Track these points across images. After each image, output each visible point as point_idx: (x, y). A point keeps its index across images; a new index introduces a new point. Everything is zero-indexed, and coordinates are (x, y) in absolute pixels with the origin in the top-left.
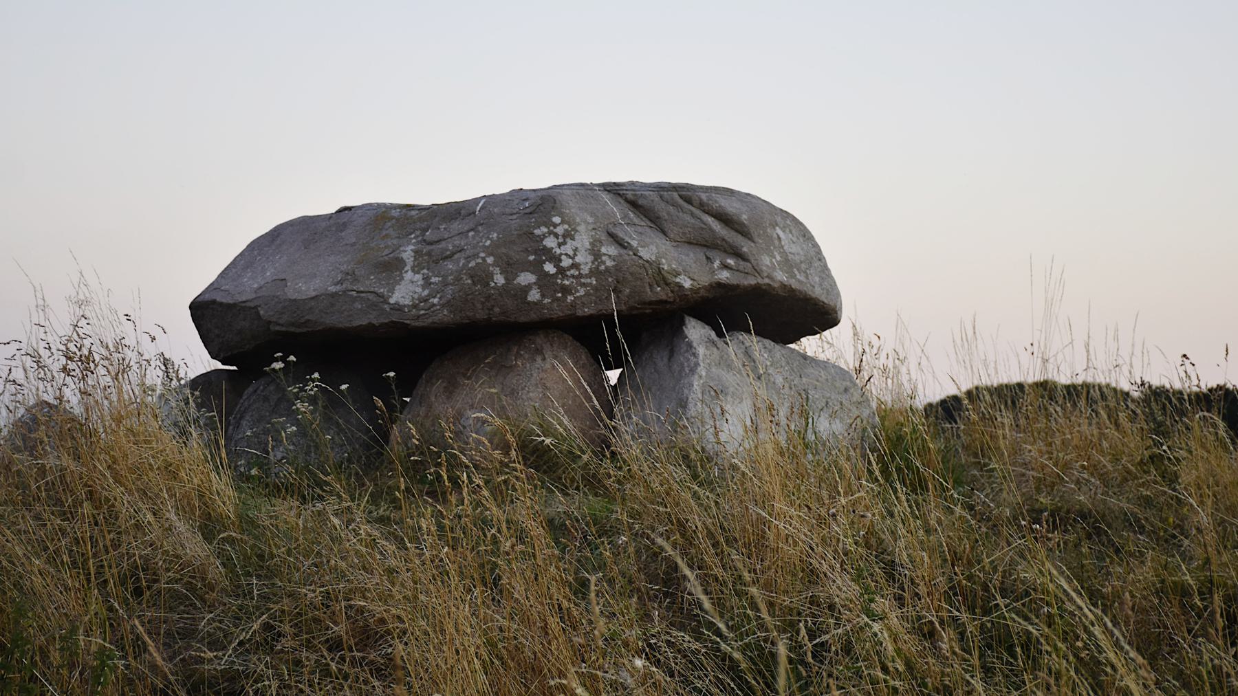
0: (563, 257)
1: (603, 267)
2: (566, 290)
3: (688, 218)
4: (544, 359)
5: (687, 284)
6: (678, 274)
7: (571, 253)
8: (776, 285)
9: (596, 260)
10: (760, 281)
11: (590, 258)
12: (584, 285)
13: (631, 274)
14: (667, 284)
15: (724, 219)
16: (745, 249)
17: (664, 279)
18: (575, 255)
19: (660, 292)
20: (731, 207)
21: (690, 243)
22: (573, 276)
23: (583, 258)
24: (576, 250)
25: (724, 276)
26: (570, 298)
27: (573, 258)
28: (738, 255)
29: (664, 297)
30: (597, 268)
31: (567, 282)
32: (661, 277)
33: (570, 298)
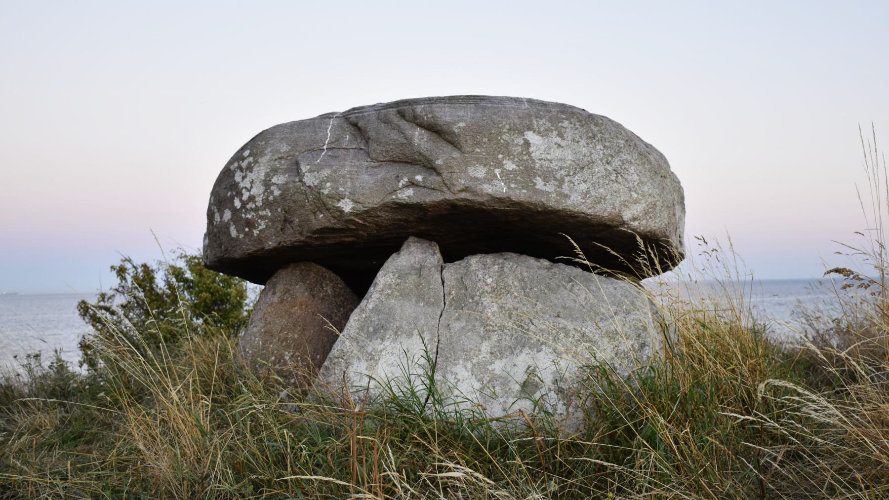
0: (244, 191)
1: (271, 198)
2: (250, 224)
3: (394, 135)
4: (274, 293)
5: (347, 206)
6: (341, 197)
7: (248, 186)
8: (480, 200)
9: (266, 190)
10: (449, 196)
11: (262, 189)
12: (262, 218)
13: (294, 202)
14: (328, 210)
15: (435, 130)
16: (439, 162)
17: (324, 204)
18: (252, 187)
19: (321, 220)
20: (444, 116)
21: (393, 161)
22: (252, 209)
23: (258, 190)
24: (252, 182)
25: (407, 195)
26: (256, 232)
27: (249, 191)
28: (431, 168)
29: (328, 224)
30: (267, 199)
31: (249, 216)
32: (321, 204)
33: (256, 232)
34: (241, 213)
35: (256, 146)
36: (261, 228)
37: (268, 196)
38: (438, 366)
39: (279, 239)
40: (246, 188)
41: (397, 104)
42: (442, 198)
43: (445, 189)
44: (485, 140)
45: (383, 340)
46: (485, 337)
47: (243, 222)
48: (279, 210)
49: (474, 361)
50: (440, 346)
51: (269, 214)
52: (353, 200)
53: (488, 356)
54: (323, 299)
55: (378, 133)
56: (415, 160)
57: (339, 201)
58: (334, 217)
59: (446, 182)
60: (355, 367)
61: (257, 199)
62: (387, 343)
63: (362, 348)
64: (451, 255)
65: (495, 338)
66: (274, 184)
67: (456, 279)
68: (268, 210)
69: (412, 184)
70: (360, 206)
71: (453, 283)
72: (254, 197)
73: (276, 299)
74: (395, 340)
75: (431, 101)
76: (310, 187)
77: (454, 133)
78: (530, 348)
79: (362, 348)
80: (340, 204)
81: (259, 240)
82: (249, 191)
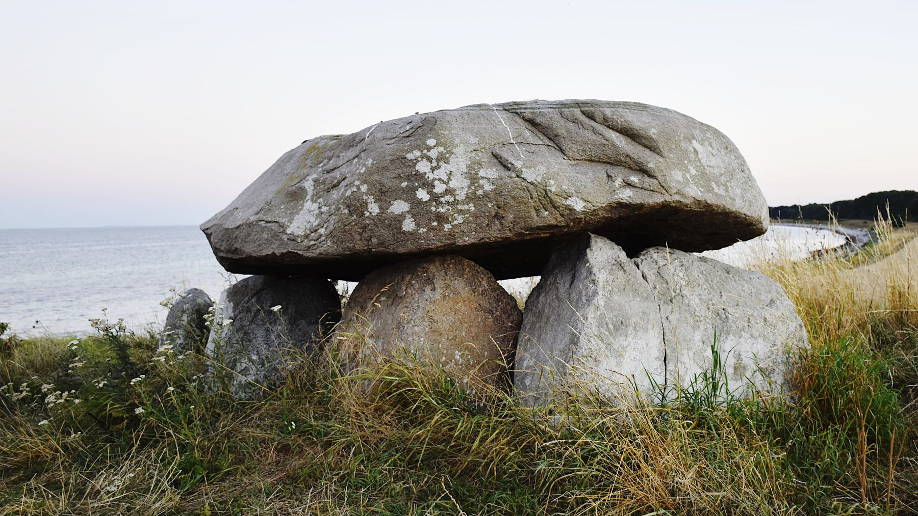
0: (436, 183)
1: (480, 192)
2: (441, 218)
3: (589, 135)
4: (434, 289)
5: (579, 206)
7: (445, 178)
8: (688, 202)
9: (473, 184)
11: (466, 183)
12: (461, 212)
13: (513, 198)
14: (555, 208)
16: (651, 165)
17: (552, 202)
18: (449, 179)
19: (548, 217)
20: (637, 121)
22: (448, 203)
23: (460, 184)
25: (626, 195)
26: (447, 227)
28: (644, 171)
29: (553, 222)
30: (474, 193)
32: (547, 200)
33: (447, 227)
35: (728, 147)
36: (456, 222)
39: (482, 235)
40: (440, 179)
41: (586, 103)
42: (663, 200)
43: (664, 192)
46: (695, 328)
47: (432, 216)
48: (490, 205)
51: (473, 209)
54: (482, 294)
55: (568, 131)
56: (621, 161)
57: (566, 199)
58: (562, 215)
61: (457, 192)
62: (630, 339)
64: (633, 252)
65: (702, 328)
68: (471, 205)
69: (629, 185)
70: (589, 205)
71: (653, 277)
72: (455, 190)
73: (438, 295)
75: (626, 105)
76: (532, 184)
77: (652, 138)
78: (734, 335)
80: (568, 202)
81: (451, 234)
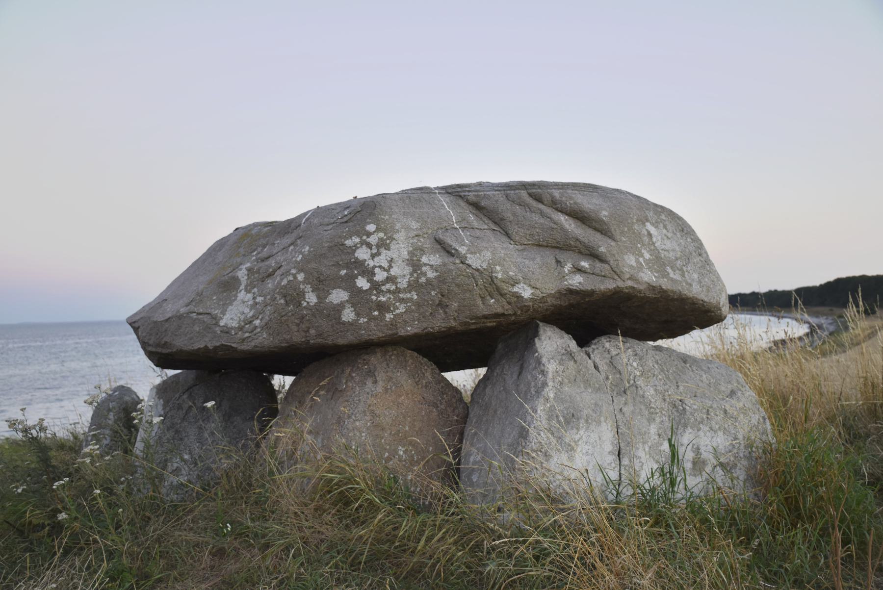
0: (377, 270)
1: (423, 280)
2: (383, 308)
3: (536, 218)
4: (375, 382)
5: (526, 293)
6: (515, 283)
8: (641, 287)
9: (415, 271)
10: (620, 284)
11: (408, 270)
12: (402, 301)
13: (458, 285)
14: (502, 295)
15: (580, 217)
16: (602, 249)
17: (498, 289)
18: (390, 267)
19: (494, 305)
20: (587, 203)
21: (539, 246)
22: (389, 291)
23: (401, 271)
24: (391, 261)
25: (576, 281)
26: (389, 316)
27: (388, 271)
28: (594, 255)
29: (500, 310)
31: (383, 299)
32: (493, 287)
33: (389, 316)
34: (371, 294)
35: (683, 228)
36: (398, 311)
37: (418, 278)
38: (623, 451)
39: (425, 325)
40: (380, 267)
41: (533, 185)
42: (615, 286)
43: (616, 277)
44: (626, 229)
45: (578, 429)
46: (650, 420)
48: (433, 293)
49: (650, 444)
50: (620, 431)
51: (416, 297)
52: (530, 285)
53: (657, 437)
54: (426, 386)
55: (514, 214)
56: (571, 246)
57: (513, 286)
58: (509, 303)
59: (616, 269)
60: (556, 460)
61: (399, 280)
62: (581, 432)
63: (560, 439)
64: (583, 341)
65: (658, 420)
66: (425, 265)
67: (606, 363)
68: (414, 293)
69: (579, 270)
70: (538, 292)
71: (606, 367)
72: (396, 278)
73: (379, 389)
74: (587, 429)
75: (575, 186)
76: (477, 270)
77: (603, 221)
78: (692, 428)
79: (560, 439)
80: (515, 289)
81: (393, 324)
82: (388, 271)
